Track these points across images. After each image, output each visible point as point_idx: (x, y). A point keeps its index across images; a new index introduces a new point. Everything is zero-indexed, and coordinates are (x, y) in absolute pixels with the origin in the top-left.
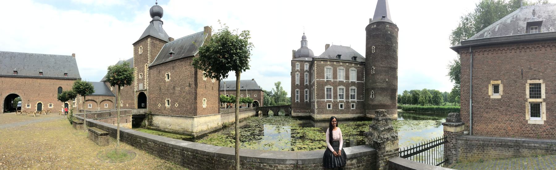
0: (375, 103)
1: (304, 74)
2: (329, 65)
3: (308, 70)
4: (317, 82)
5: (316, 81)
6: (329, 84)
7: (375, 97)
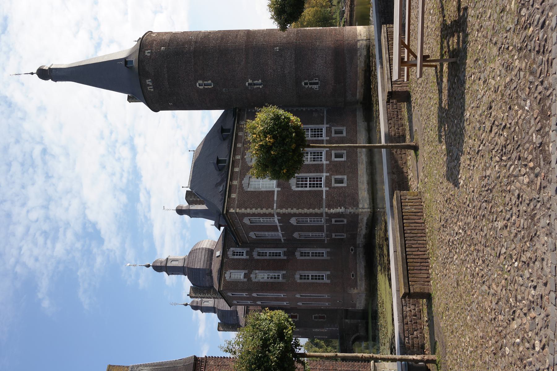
1: (258, 260)
2: (241, 182)
3: (248, 249)
4: (280, 207)
5: (278, 210)
7: (317, 76)
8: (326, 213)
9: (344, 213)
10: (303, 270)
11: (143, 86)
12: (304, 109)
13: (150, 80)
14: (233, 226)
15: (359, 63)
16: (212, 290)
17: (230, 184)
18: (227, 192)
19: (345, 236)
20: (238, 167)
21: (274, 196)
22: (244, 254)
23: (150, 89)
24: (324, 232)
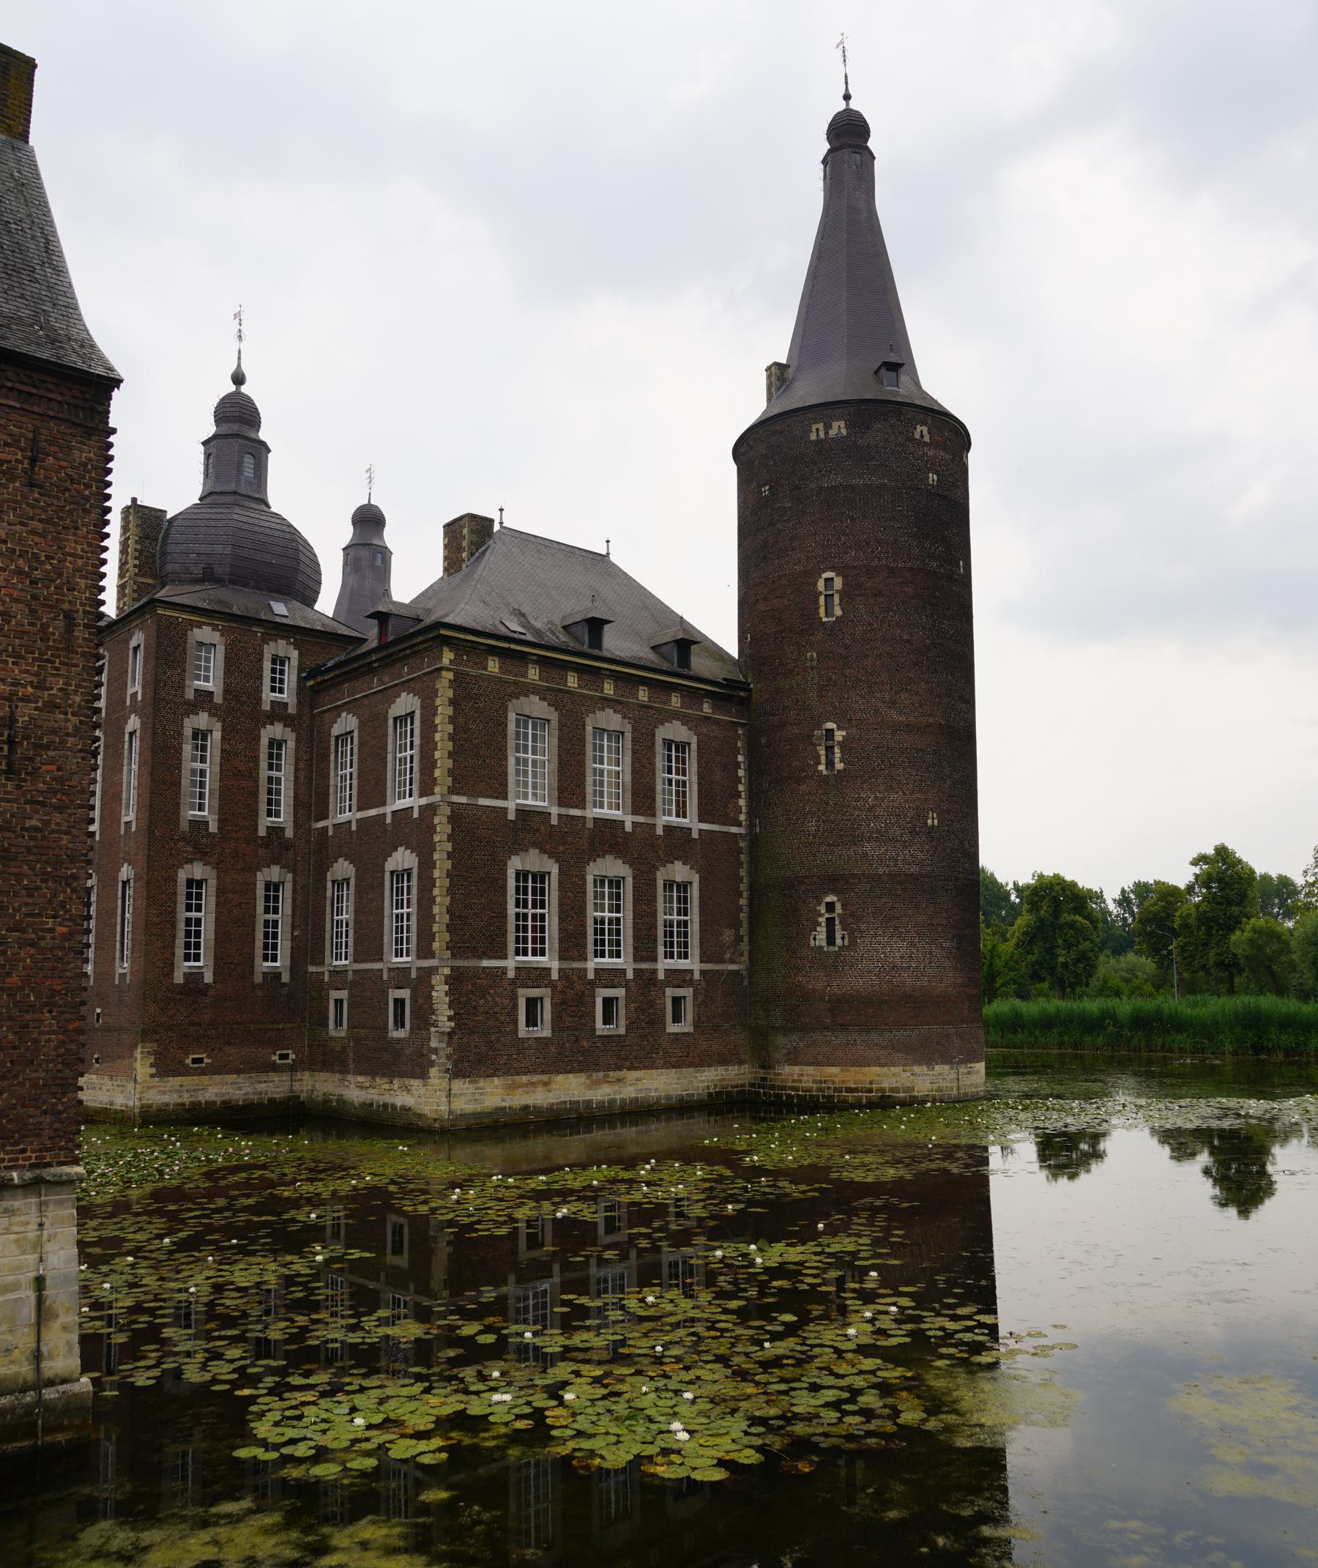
0: (858, 981)
1: (257, 739)
3: (292, 710)
4: (457, 816)
6: (535, 845)
7: (853, 942)
8: (432, 971)
9: (433, 1029)
10: (220, 891)
11: (824, 410)
12: (743, 902)
13: (844, 432)
14: (387, 661)
15: (893, 1069)
16: (150, 581)
17: (530, 657)
18: (506, 645)
19: (337, 1031)
20: (580, 687)
21: (491, 797)
22: (277, 695)
23: (817, 429)
24: (355, 961)
